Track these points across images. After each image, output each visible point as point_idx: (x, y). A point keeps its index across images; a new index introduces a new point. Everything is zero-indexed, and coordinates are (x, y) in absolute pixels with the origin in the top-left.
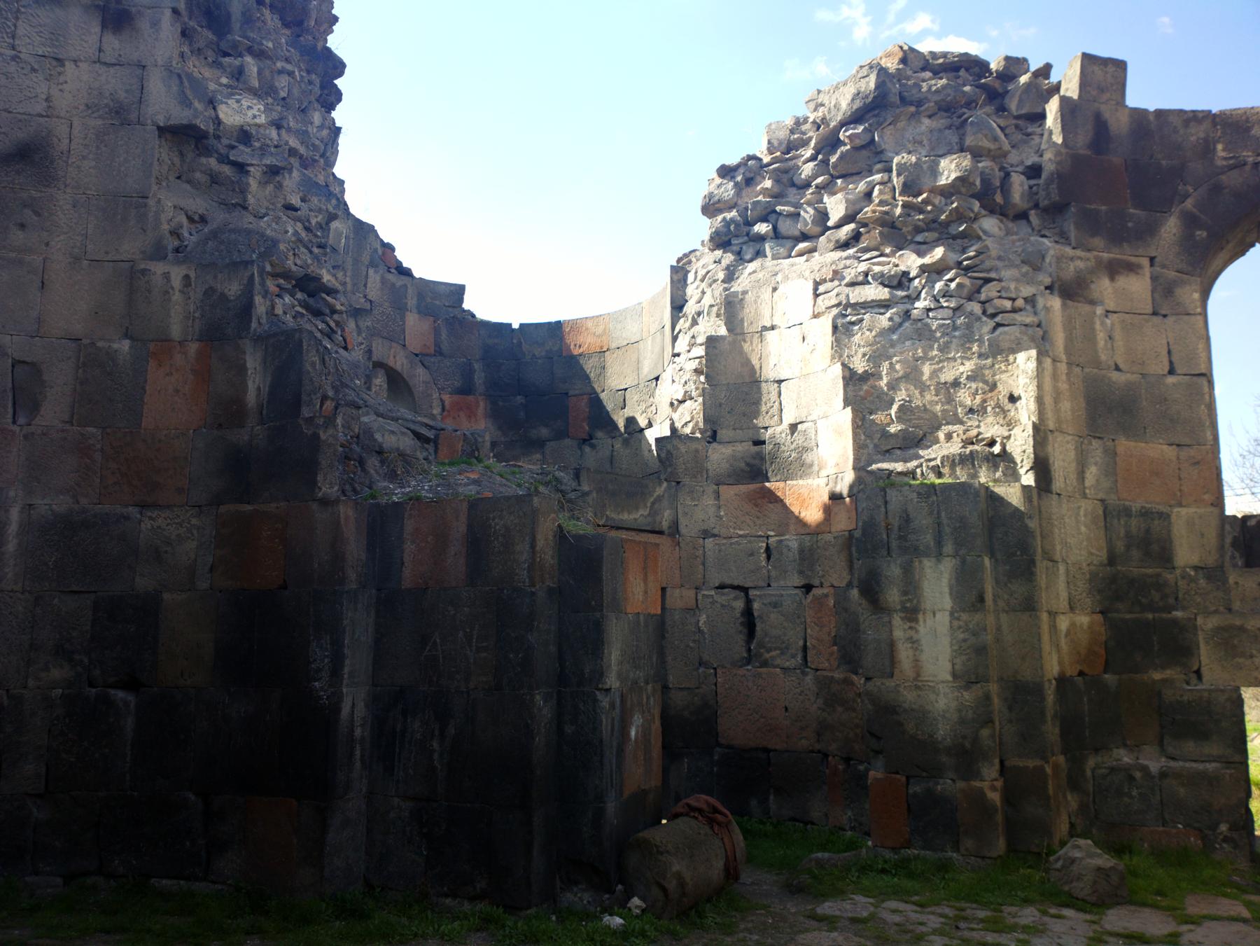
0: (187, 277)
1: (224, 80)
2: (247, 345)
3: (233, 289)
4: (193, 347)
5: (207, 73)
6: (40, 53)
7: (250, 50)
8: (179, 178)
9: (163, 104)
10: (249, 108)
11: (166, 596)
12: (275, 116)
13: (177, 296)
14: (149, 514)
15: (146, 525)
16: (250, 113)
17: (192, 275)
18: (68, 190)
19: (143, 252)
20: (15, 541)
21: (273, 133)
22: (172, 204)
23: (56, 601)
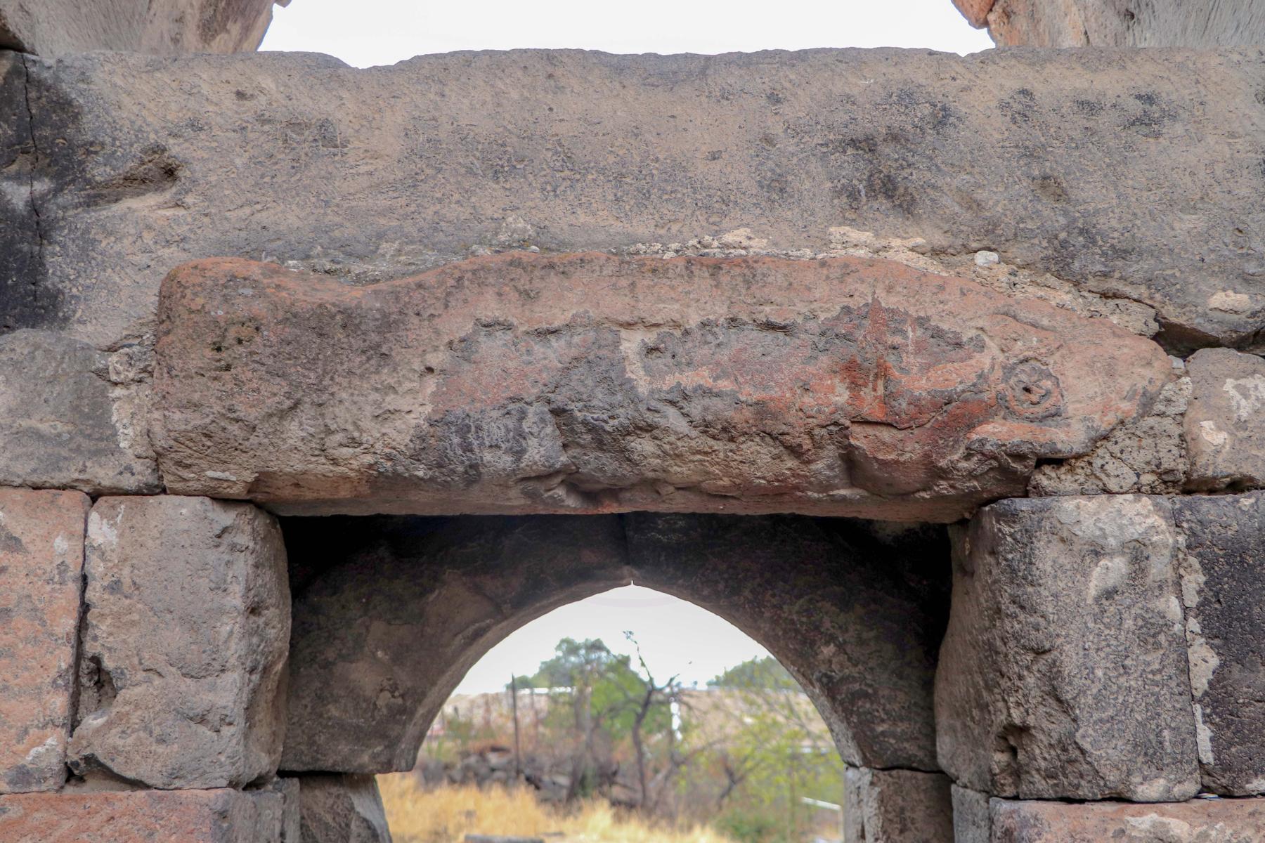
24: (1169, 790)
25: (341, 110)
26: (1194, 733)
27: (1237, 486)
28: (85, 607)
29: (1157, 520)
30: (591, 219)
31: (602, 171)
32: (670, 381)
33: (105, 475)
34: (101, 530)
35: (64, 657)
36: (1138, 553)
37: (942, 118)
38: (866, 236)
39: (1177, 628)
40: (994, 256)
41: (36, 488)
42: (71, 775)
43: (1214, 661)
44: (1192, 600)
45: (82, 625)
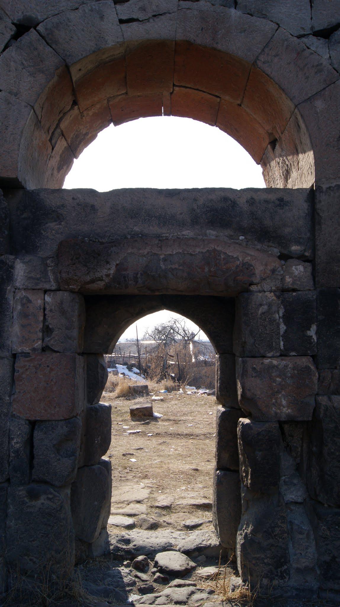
24: (273, 355)
26: (280, 343)
27: (294, 290)
28: (45, 315)
29: (274, 298)
31: (156, 217)
32: (169, 267)
33: (47, 287)
34: (48, 298)
35: (41, 326)
36: (270, 305)
37: (234, 204)
38: (214, 233)
39: (277, 321)
40: (243, 237)
41: (34, 289)
43: (285, 328)
44: (281, 314)
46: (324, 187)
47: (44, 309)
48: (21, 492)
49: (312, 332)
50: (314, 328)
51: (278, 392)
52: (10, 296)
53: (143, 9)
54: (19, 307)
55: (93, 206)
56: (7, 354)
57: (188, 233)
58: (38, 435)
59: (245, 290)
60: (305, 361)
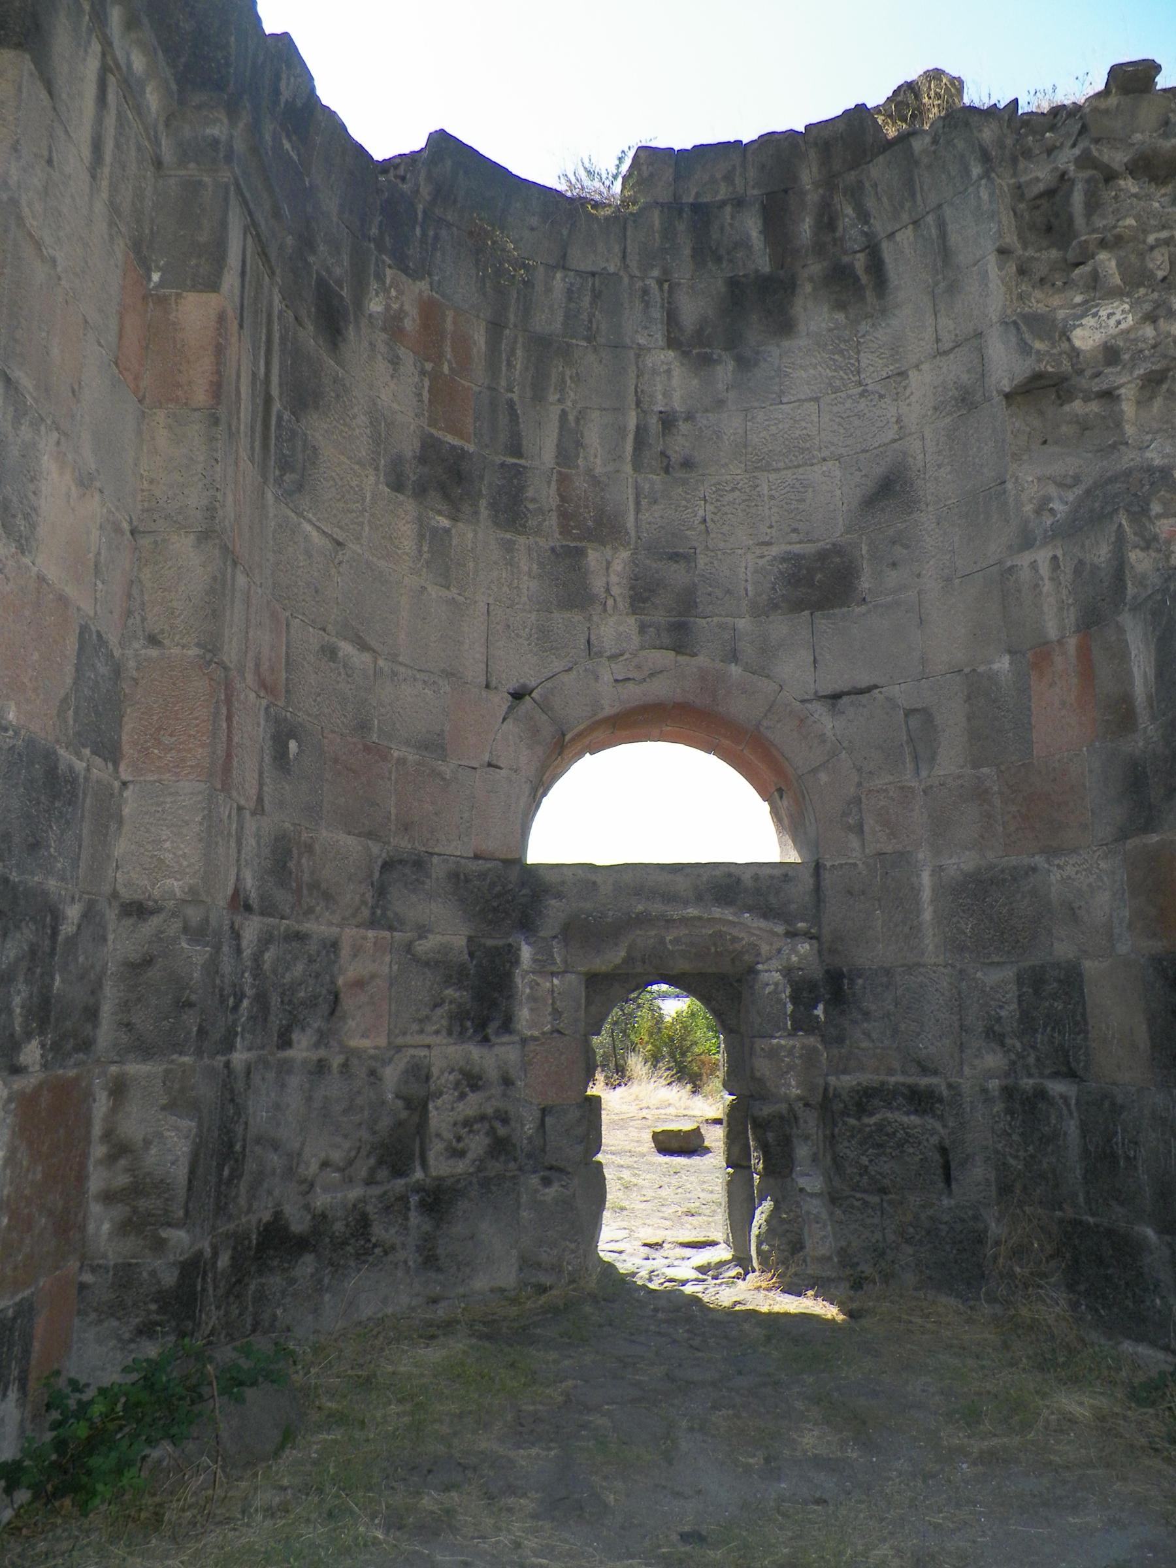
0: (1055, 558)
1: (1078, 299)
2: (1127, 619)
3: (1101, 554)
4: (1072, 642)
5: (1056, 301)
6: (885, 375)
7: (1103, 244)
8: (1045, 442)
9: (1005, 364)
10: (1109, 316)
11: (1087, 964)
12: (1147, 307)
13: (1047, 586)
14: (1057, 862)
15: (1055, 876)
16: (1112, 322)
17: (1059, 553)
18: (930, 509)
19: (1010, 547)
20: (931, 909)
21: (1149, 331)
22: (1042, 480)
23: (979, 974)
25: (599, 879)
30: (656, 908)
33: (555, 969)
34: (556, 981)
35: (550, 1009)
36: (776, 984)
37: (739, 881)
42: (552, 1032)
45: (553, 1004)
46: (828, 864)
47: (553, 991)
48: (534, 1180)
49: (819, 1011)
50: (821, 1007)
51: (787, 1072)
52: (518, 980)
53: (639, 667)
54: (528, 991)
55: (594, 883)
56: (517, 1038)
57: (692, 911)
58: (549, 1121)
59: (752, 971)
60: (812, 1041)
